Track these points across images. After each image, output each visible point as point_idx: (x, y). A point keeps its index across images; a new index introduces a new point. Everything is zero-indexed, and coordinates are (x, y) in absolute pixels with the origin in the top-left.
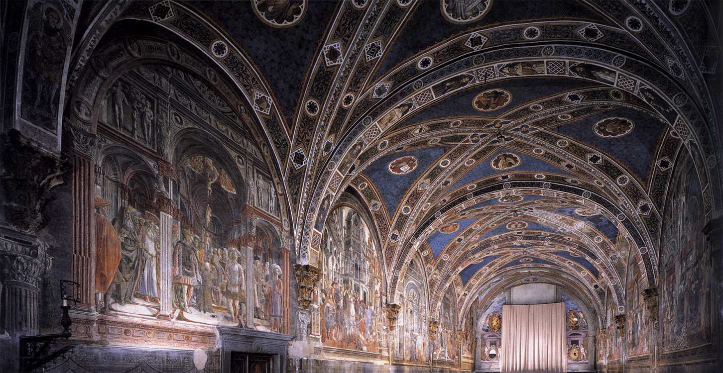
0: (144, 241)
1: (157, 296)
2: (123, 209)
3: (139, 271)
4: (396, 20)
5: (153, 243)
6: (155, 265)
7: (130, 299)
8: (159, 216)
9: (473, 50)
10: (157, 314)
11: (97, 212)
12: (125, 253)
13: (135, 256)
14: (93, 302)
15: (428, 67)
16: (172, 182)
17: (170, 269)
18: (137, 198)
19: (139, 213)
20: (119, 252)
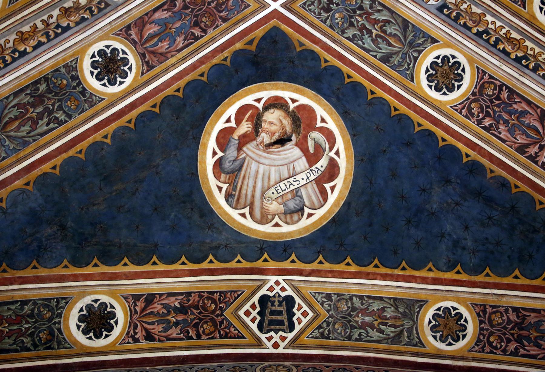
4: (61, 116)
9: (259, 344)
15: (101, 343)
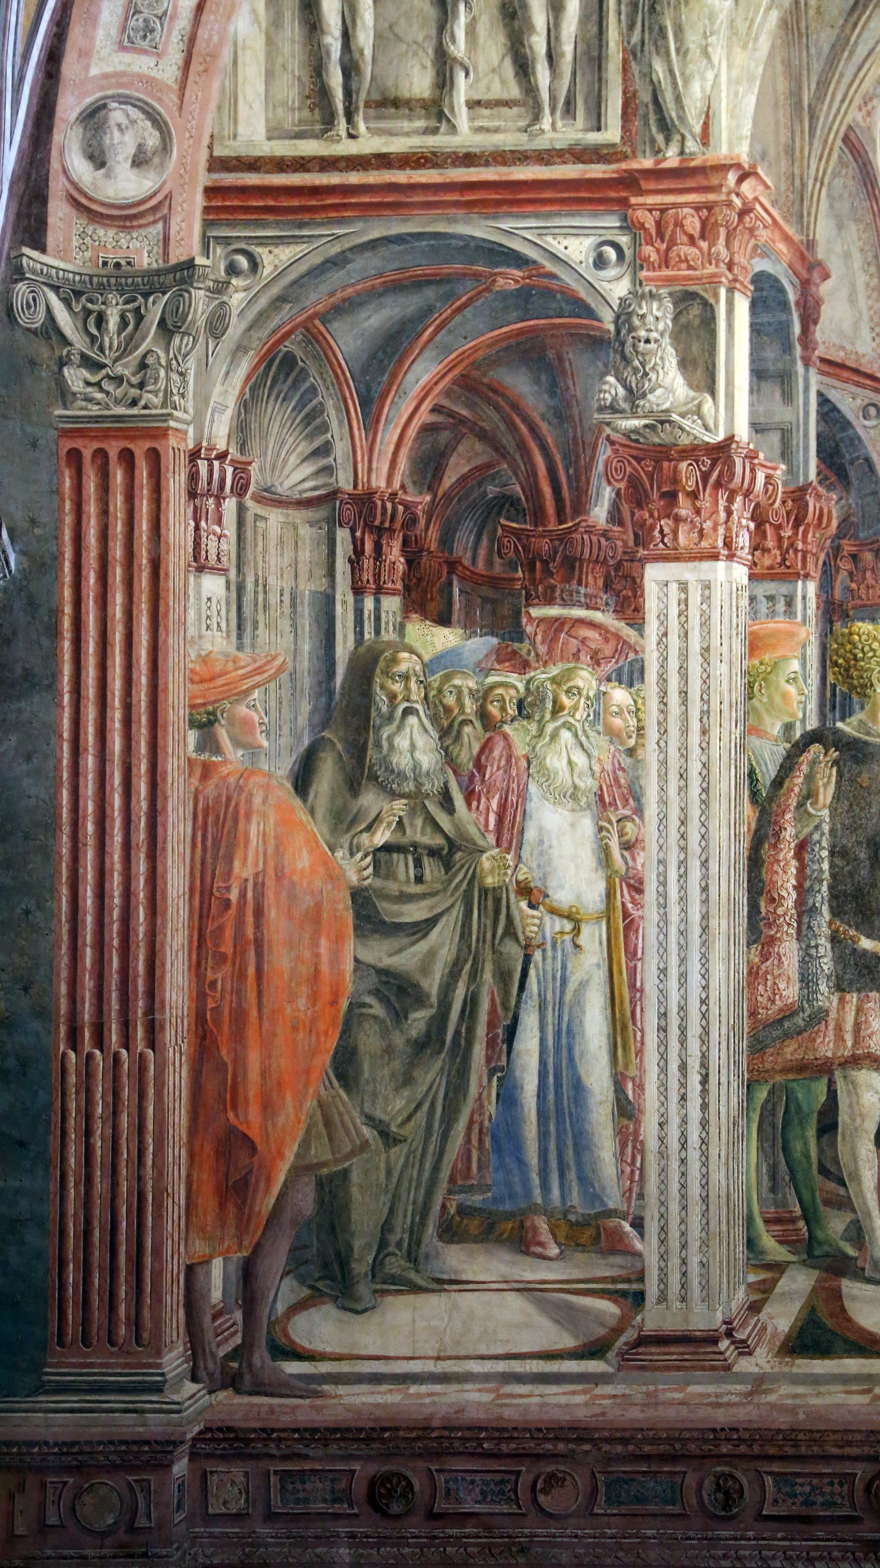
0: (510, 826)
1: (614, 1201)
2: (367, 667)
3: (479, 1051)
5: (587, 825)
6: (600, 976)
7: (413, 1257)
8: (630, 605)
10: (617, 1331)
11: (201, 747)
12: (380, 953)
13: (446, 955)
14: (175, 1318)
16: (742, 306)
17: (725, 966)
18: (463, 544)
19: (481, 645)
20: (336, 959)
